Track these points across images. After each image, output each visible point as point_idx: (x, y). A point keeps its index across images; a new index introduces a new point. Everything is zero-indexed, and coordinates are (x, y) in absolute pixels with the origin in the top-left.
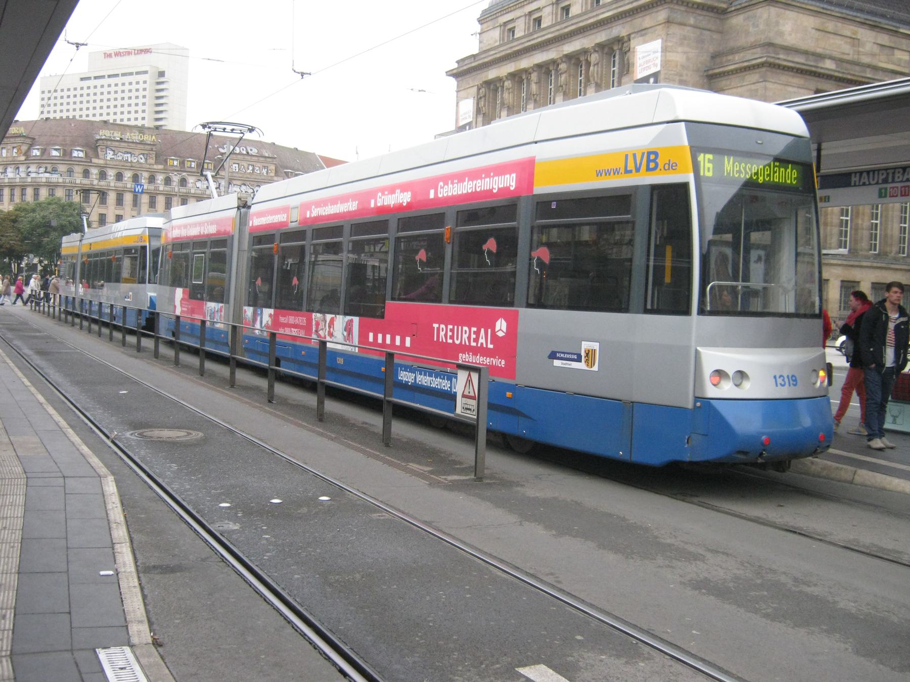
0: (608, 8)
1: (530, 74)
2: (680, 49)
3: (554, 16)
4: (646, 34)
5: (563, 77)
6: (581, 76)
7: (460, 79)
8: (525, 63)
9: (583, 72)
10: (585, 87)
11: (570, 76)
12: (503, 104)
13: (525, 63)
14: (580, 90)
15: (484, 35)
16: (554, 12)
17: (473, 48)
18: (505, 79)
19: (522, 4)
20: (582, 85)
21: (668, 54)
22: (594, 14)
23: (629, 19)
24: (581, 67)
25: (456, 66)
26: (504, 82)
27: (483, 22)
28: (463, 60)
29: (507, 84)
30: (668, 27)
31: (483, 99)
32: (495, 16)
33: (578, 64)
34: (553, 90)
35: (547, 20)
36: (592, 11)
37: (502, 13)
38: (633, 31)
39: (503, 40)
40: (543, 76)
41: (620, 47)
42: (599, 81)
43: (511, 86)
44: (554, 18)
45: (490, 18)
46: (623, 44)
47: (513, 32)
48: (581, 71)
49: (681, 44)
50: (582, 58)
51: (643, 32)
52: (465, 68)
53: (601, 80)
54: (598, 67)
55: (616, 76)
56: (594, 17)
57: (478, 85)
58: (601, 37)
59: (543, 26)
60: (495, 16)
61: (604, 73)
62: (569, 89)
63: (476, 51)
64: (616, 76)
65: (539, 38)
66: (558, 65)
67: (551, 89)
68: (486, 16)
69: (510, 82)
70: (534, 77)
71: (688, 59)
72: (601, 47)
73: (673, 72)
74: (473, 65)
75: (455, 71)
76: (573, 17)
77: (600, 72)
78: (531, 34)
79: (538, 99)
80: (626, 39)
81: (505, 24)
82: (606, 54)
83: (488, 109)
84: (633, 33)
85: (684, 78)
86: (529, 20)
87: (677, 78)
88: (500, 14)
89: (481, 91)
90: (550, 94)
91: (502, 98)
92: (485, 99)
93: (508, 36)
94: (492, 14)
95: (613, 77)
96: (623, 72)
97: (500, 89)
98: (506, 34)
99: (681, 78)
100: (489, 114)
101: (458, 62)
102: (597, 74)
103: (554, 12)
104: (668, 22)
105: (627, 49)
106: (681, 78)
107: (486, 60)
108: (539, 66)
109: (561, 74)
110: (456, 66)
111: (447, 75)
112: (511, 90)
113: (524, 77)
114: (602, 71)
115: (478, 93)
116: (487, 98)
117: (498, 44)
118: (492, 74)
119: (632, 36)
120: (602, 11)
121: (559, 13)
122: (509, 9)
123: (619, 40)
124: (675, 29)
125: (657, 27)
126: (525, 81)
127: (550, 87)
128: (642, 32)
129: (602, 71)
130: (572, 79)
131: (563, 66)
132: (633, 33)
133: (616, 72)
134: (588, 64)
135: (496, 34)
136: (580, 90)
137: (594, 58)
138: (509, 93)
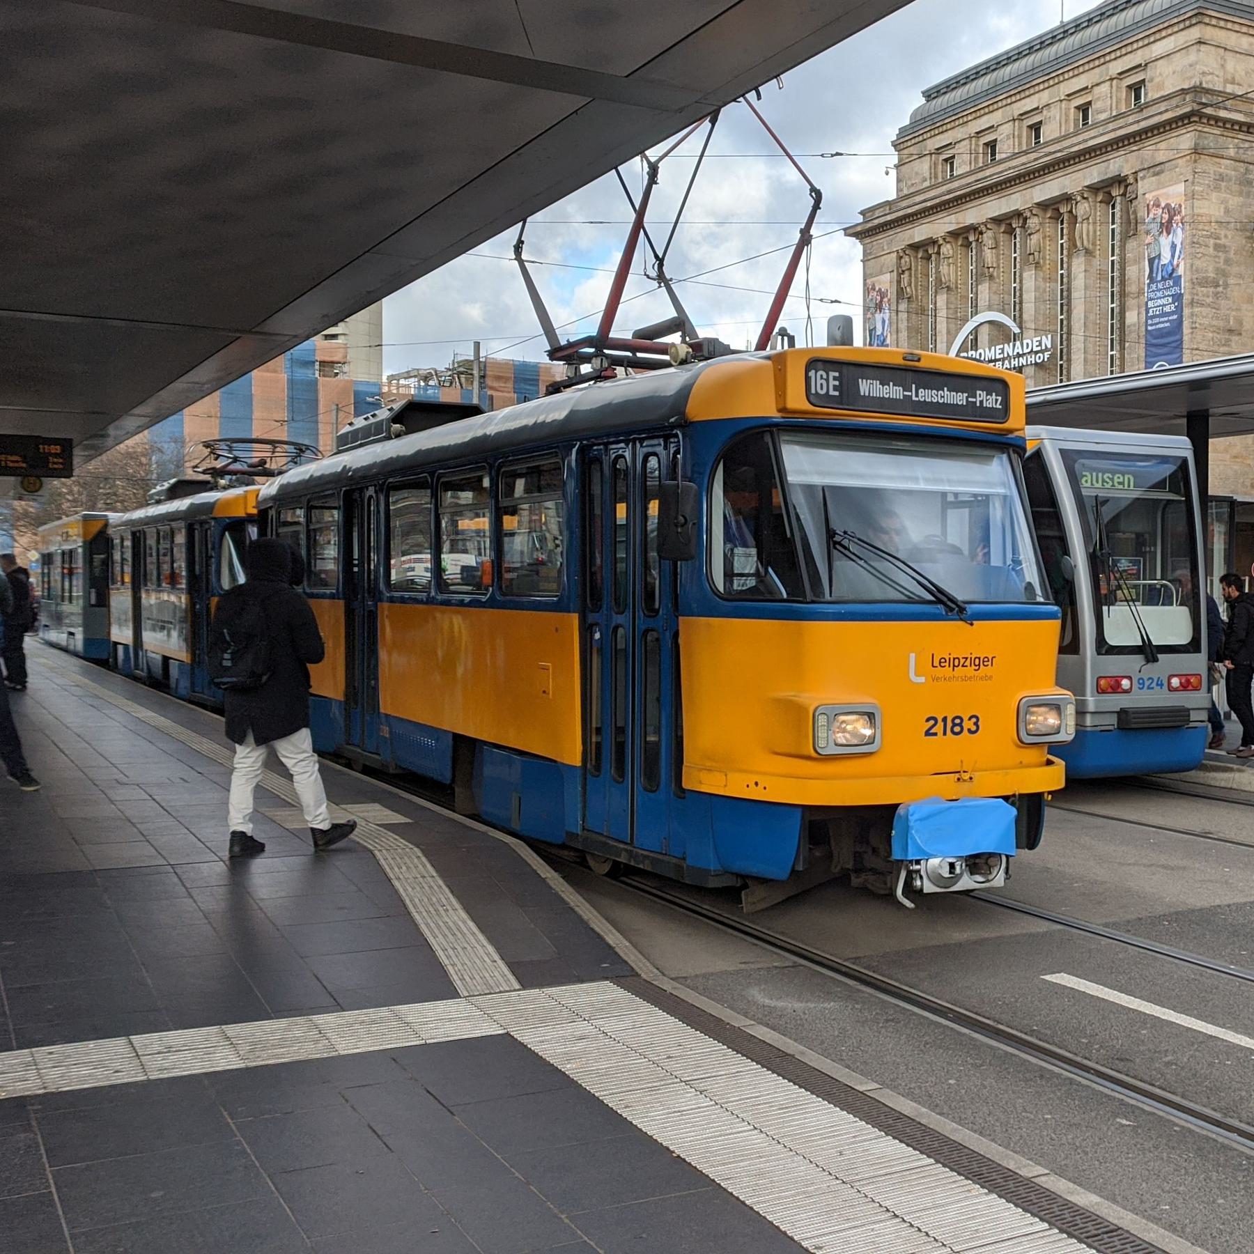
0: (1101, 130)
1: (981, 233)
2: (1214, 195)
3: (1016, 140)
4: (1162, 172)
5: (1034, 237)
6: (1062, 239)
7: (868, 240)
8: (973, 215)
9: (1065, 231)
10: (1070, 256)
11: (1044, 238)
12: (939, 281)
13: (973, 215)
14: (1062, 259)
15: (903, 168)
16: (1016, 133)
17: (889, 191)
18: (941, 242)
19: (965, 119)
20: (1065, 252)
21: (1196, 203)
22: (1080, 138)
23: (1135, 148)
24: (1062, 223)
25: (860, 219)
26: (939, 246)
27: (902, 146)
28: (872, 209)
29: (946, 249)
30: (1195, 161)
31: (907, 273)
32: (921, 138)
33: (1057, 217)
34: (1018, 260)
35: (1005, 147)
36: (1076, 134)
37: (933, 133)
38: (1141, 167)
39: (936, 177)
40: (1002, 237)
41: (1121, 192)
42: (1091, 247)
43: (951, 252)
44: (1016, 144)
45: (913, 141)
46: (1126, 187)
47: (952, 164)
48: (1062, 229)
49: (1217, 188)
50: (1063, 209)
51: (1158, 169)
52: (876, 222)
53: (1094, 244)
54: (1089, 223)
55: (1117, 237)
56: (1079, 143)
57: (897, 251)
58: (1093, 173)
59: (998, 157)
60: (921, 138)
61: (1098, 233)
62: (1044, 258)
63: (892, 195)
64: (1117, 237)
65: (994, 173)
66: (1025, 219)
67: (1015, 258)
68: (907, 138)
69: (948, 246)
70: (988, 238)
71: (1227, 211)
72: (1094, 189)
73: (1205, 233)
74: (889, 218)
75: (859, 229)
76: (1047, 144)
77: (1091, 233)
78: (981, 169)
79: (995, 274)
80: (1131, 180)
81: (939, 150)
82: (1100, 202)
83: (916, 290)
84: (1140, 170)
85: (1223, 241)
86: (977, 145)
87: (1212, 241)
88: (929, 135)
89: (903, 261)
90: (1015, 268)
91: (938, 272)
92: (910, 275)
93: (944, 171)
94: (917, 134)
95: (1113, 240)
96: (1127, 232)
97: (933, 257)
98: (940, 167)
99: (1218, 241)
100: (917, 296)
101: (863, 213)
102: (1088, 235)
103: (1016, 133)
104: (1197, 151)
105: (1134, 196)
106: (1218, 241)
107: (910, 211)
108: (997, 221)
109: (1030, 235)
110: (860, 219)
111: (846, 235)
112: (951, 260)
113: (971, 238)
114: (1095, 231)
115: (899, 266)
116: (913, 272)
117: (927, 184)
118: (920, 232)
119: (1141, 175)
120: (1093, 133)
121: (1024, 134)
122: (944, 128)
123: (1120, 180)
124: (1206, 164)
125: (1180, 161)
126: (974, 245)
127: (1014, 255)
128: (1156, 168)
129: (1095, 231)
130: (1048, 243)
131: (1033, 222)
132: (1140, 170)
133: (1117, 231)
134: (1074, 219)
135: (923, 167)
136: (1062, 259)
137: (1082, 209)
138: (949, 265)
